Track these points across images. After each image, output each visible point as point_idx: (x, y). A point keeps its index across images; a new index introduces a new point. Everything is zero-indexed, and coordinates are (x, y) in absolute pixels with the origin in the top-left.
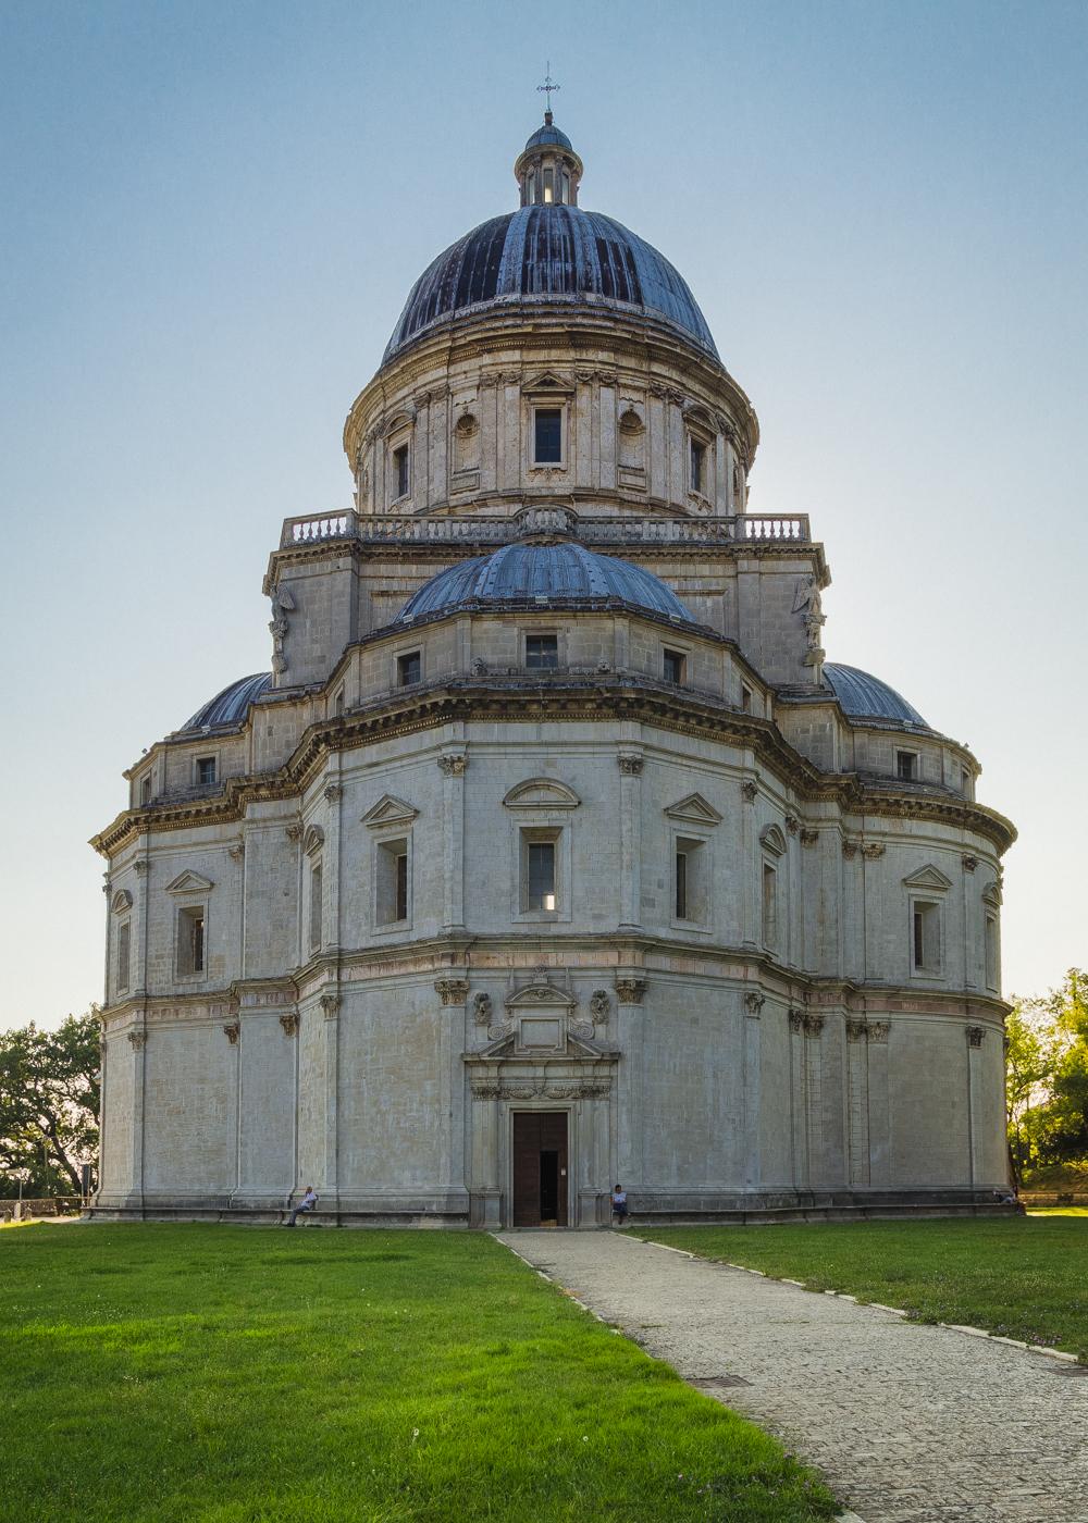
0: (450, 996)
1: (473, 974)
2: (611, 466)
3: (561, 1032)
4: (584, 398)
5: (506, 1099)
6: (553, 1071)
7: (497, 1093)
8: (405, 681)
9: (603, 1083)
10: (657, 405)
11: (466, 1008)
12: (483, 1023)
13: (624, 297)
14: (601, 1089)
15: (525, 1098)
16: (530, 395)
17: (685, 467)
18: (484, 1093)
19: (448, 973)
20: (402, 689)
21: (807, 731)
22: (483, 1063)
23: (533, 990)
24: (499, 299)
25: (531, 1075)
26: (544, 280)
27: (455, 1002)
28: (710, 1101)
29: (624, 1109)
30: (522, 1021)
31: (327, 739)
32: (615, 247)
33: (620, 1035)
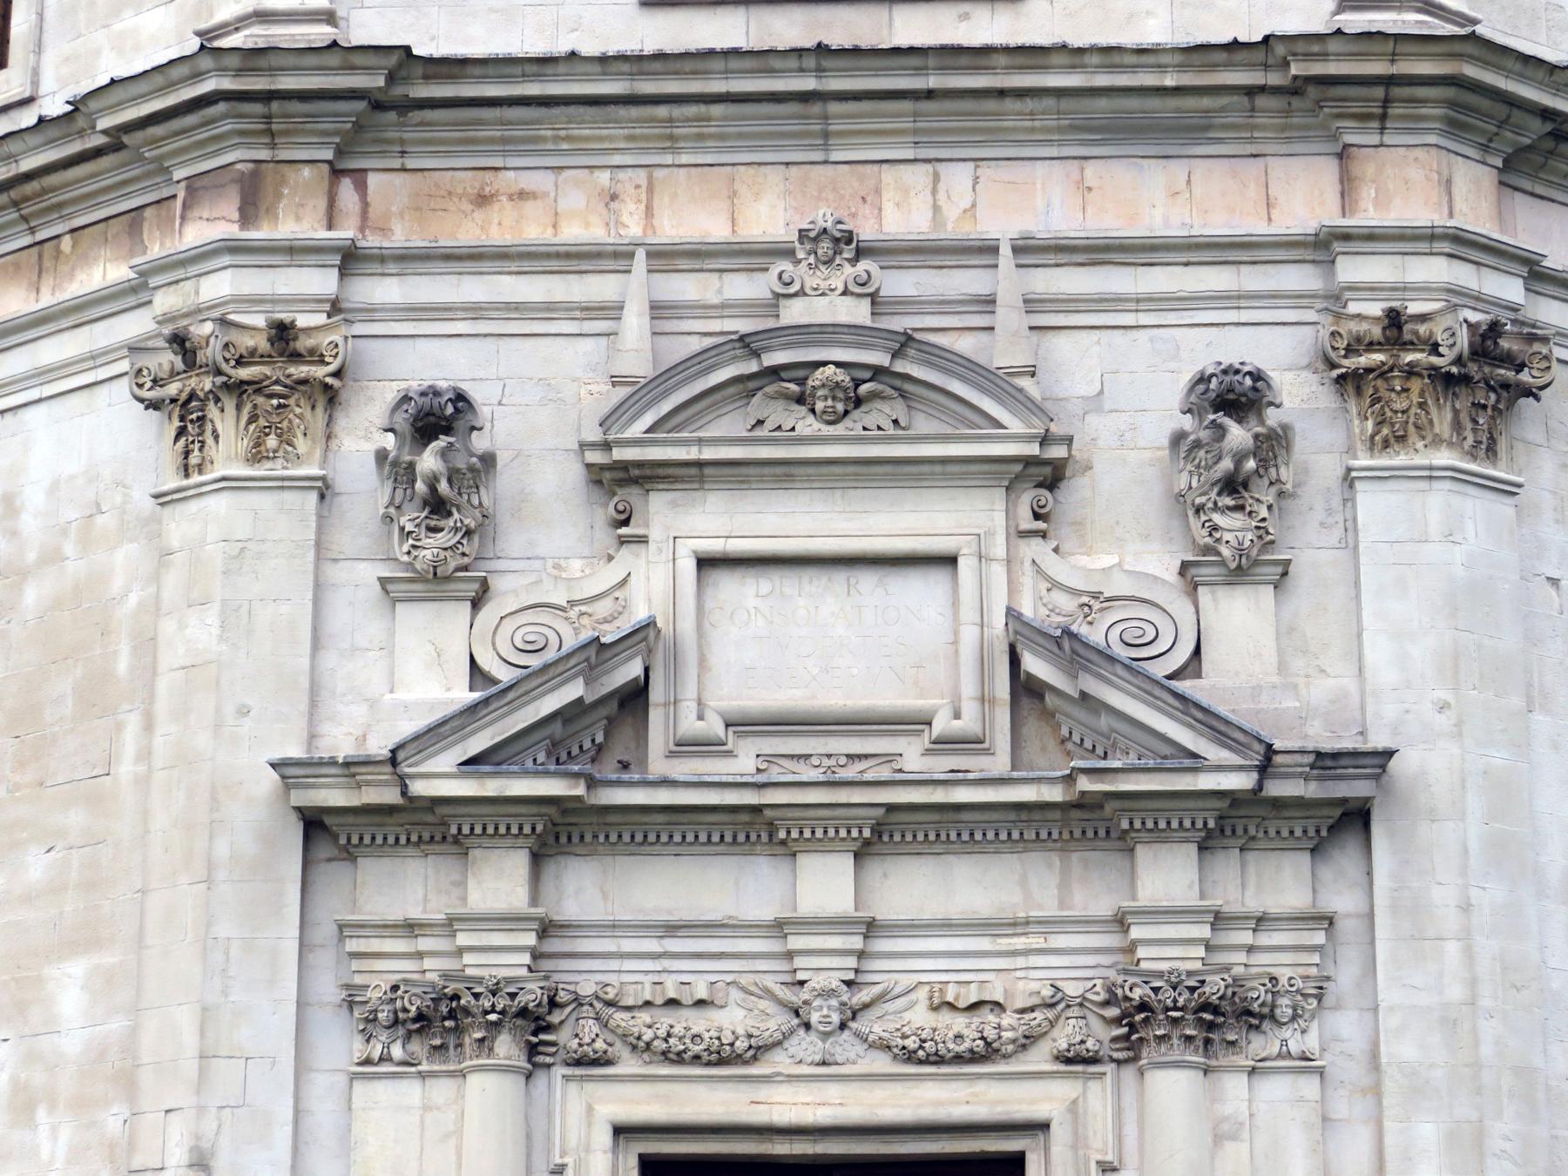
0: (226, 422)
3: (969, 635)
5: (589, 1061)
6: (913, 887)
7: (538, 1029)
9: (1278, 959)
11: (324, 490)
12: (433, 582)
14: (1258, 993)
15: (722, 1058)
18: (436, 1023)
19: (219, 285)
22: (435, 828)
23: (769, 372)
25: (765, 910)
27: (257, 455)
29: (1427, 1131)
30: (706, 563)
33: (1377, 651)
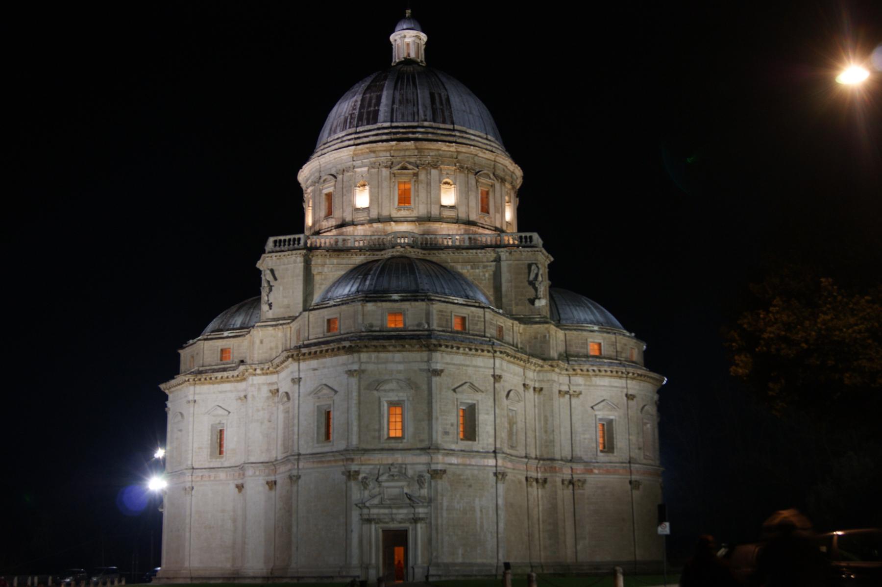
1: (363, 467)
2: (438, 207)
4: (422, 176)
5: (377, 523)
8: (329, 330)
10: (461, 177)
13: (444, 122)
15: (387, 523)
16: (394, 174)
17: (477, 204)
18: (369, 521)
20: (329, 334)
21: (536, 338)
24: (379, 125)
26: (403, 116)
28: (478, 523)
31: (292, 356)
32: (440, 95)
